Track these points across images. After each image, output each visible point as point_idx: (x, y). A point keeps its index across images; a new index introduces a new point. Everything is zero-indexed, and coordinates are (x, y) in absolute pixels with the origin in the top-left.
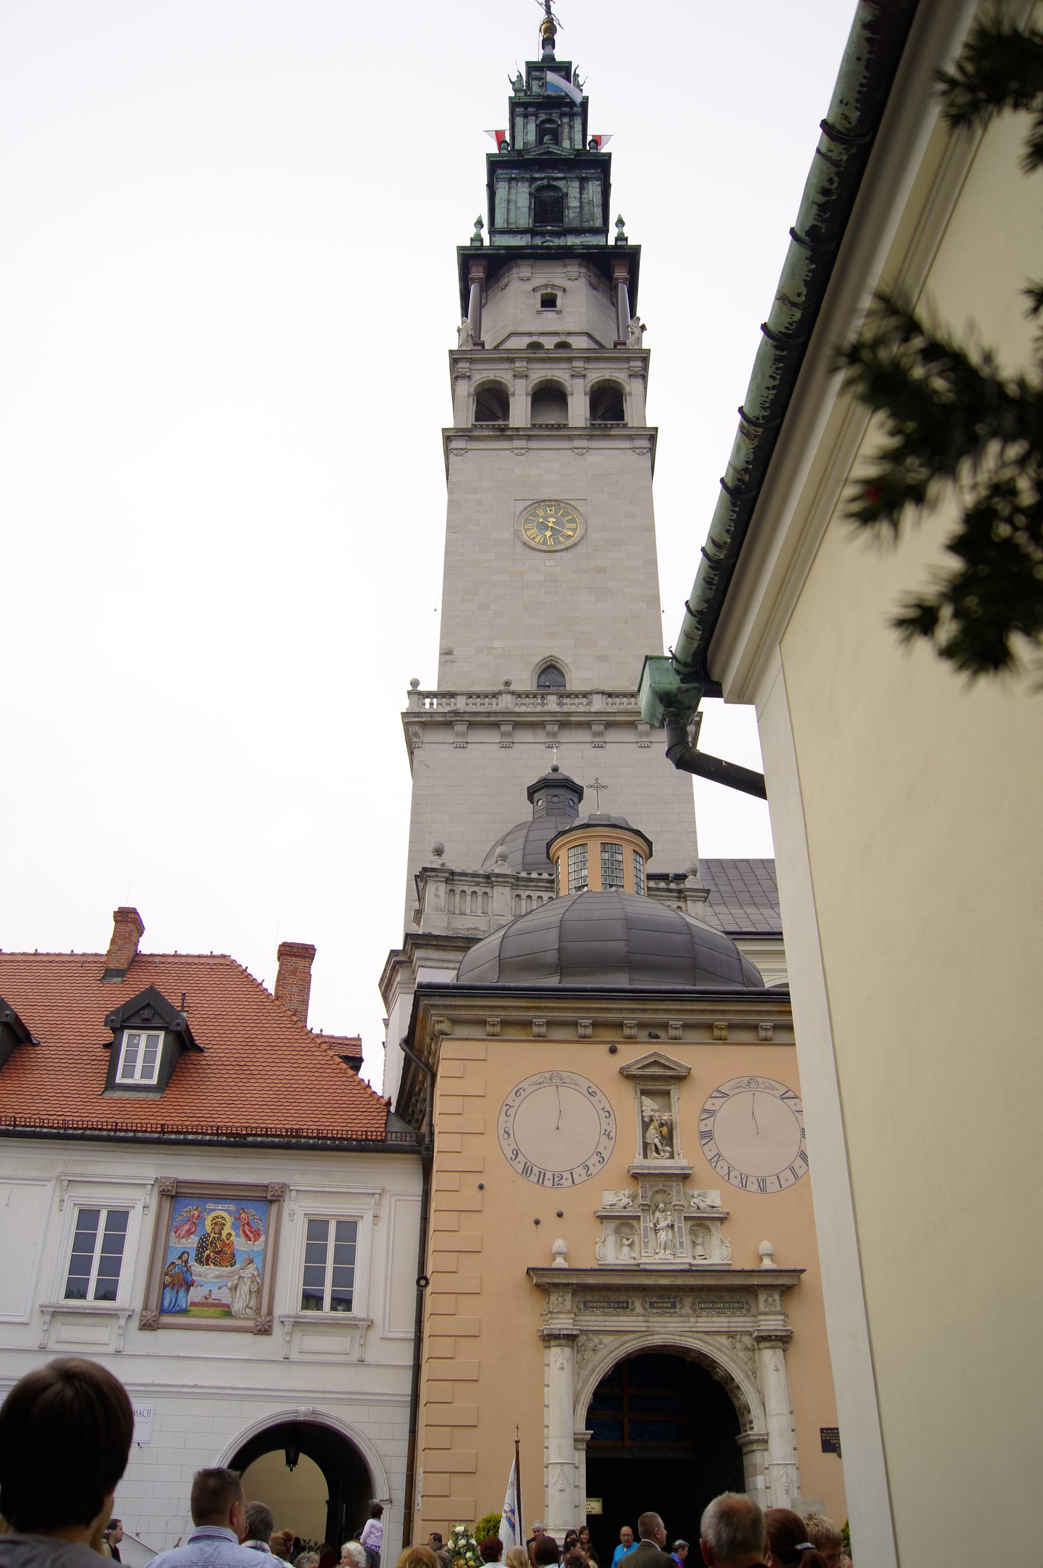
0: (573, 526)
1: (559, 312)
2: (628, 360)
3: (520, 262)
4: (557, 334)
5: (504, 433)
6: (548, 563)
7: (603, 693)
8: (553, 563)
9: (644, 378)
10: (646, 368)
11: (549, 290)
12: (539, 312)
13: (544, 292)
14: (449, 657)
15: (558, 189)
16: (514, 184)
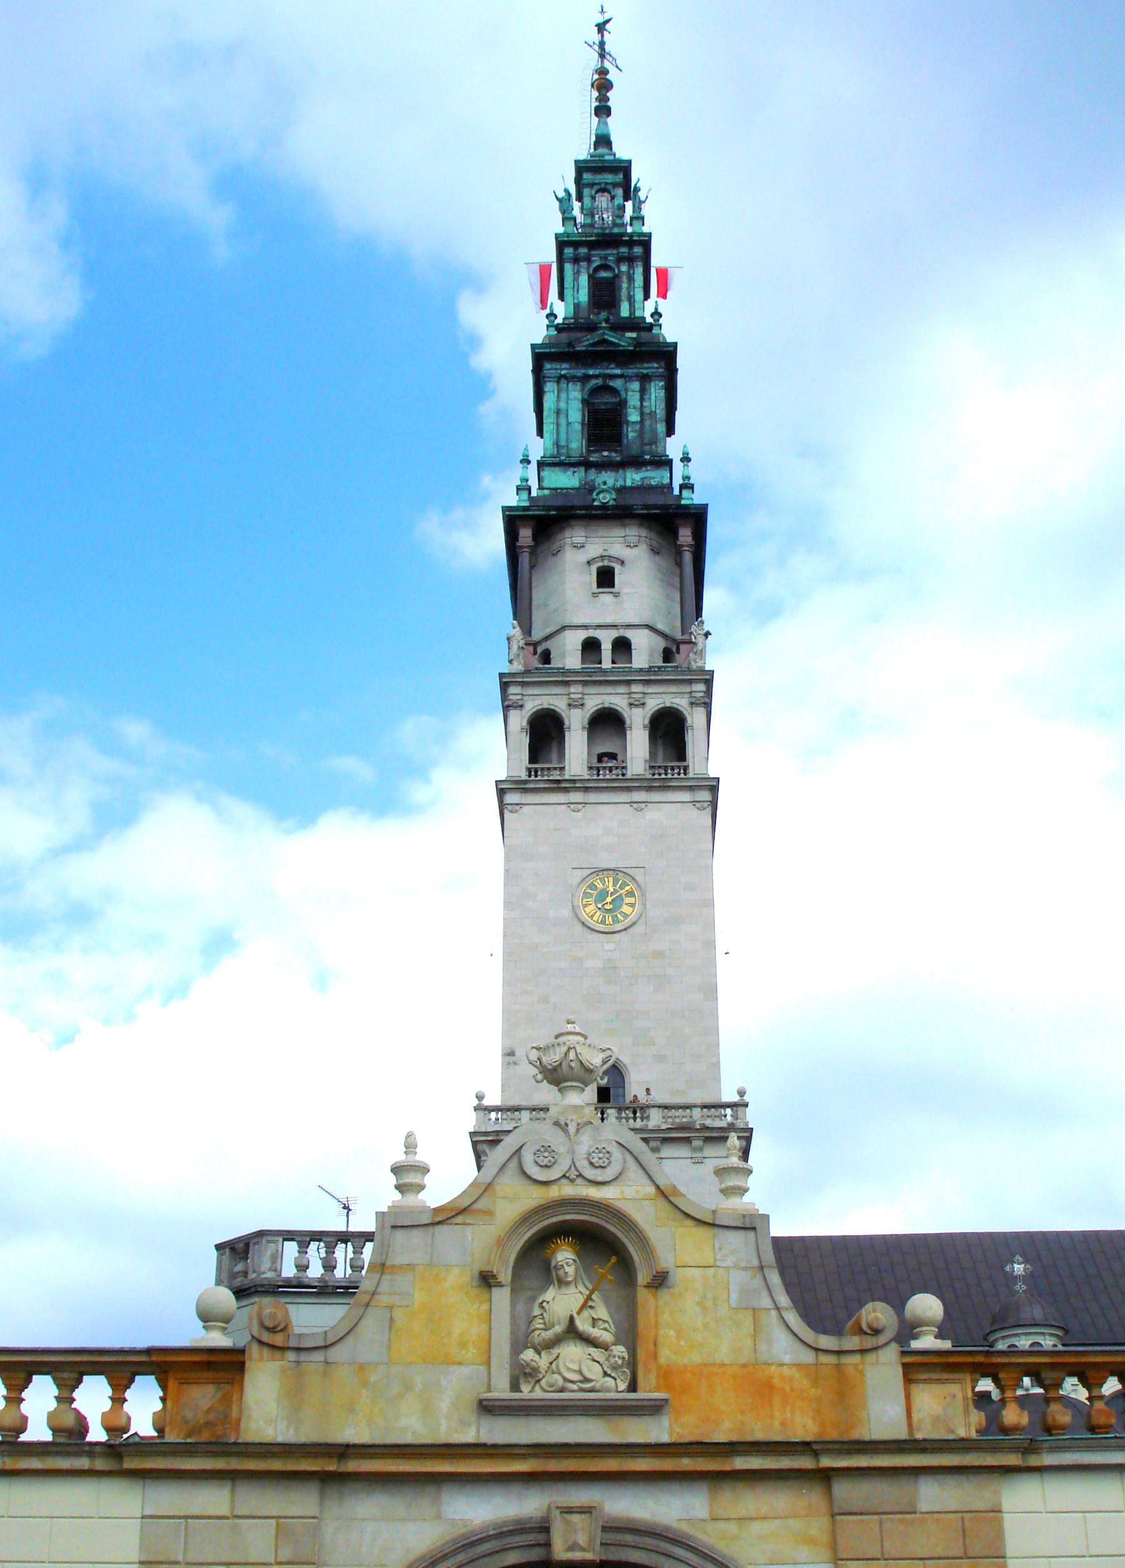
0: (632, 900)
1: (616, 595)
2: (690, 682)
3: (573, 522)
4: (615, 626)
5: (559, 786)
6: (607, 947)
7: (659, 1107)
8: (611, 946)
9: (708, 706)
10: (709, 693)
11: (606, 563)
12: (595, 595)
13: (600, 564)
14: (511, 1059)
15: (614, 391)
16: (563, 384)
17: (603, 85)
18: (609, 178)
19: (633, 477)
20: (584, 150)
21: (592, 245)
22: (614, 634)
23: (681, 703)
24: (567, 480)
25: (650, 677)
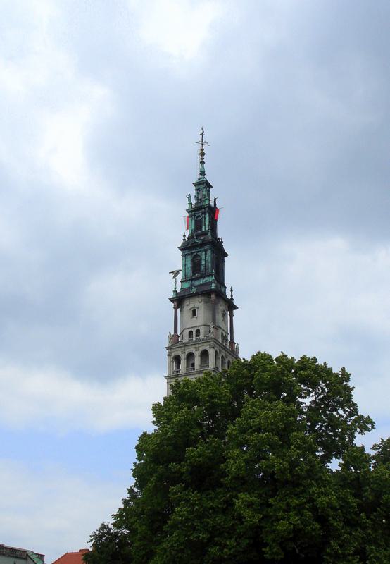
12: (192, 319)
17: (203, 154)
18: (202, 186)
19: (202, 281)
20: (195, 180)
21: (195, 211)
22: (196, 329)
23: (207, 348)
24: (187, 285)
25: (199, 342)
